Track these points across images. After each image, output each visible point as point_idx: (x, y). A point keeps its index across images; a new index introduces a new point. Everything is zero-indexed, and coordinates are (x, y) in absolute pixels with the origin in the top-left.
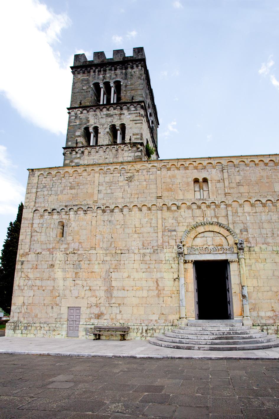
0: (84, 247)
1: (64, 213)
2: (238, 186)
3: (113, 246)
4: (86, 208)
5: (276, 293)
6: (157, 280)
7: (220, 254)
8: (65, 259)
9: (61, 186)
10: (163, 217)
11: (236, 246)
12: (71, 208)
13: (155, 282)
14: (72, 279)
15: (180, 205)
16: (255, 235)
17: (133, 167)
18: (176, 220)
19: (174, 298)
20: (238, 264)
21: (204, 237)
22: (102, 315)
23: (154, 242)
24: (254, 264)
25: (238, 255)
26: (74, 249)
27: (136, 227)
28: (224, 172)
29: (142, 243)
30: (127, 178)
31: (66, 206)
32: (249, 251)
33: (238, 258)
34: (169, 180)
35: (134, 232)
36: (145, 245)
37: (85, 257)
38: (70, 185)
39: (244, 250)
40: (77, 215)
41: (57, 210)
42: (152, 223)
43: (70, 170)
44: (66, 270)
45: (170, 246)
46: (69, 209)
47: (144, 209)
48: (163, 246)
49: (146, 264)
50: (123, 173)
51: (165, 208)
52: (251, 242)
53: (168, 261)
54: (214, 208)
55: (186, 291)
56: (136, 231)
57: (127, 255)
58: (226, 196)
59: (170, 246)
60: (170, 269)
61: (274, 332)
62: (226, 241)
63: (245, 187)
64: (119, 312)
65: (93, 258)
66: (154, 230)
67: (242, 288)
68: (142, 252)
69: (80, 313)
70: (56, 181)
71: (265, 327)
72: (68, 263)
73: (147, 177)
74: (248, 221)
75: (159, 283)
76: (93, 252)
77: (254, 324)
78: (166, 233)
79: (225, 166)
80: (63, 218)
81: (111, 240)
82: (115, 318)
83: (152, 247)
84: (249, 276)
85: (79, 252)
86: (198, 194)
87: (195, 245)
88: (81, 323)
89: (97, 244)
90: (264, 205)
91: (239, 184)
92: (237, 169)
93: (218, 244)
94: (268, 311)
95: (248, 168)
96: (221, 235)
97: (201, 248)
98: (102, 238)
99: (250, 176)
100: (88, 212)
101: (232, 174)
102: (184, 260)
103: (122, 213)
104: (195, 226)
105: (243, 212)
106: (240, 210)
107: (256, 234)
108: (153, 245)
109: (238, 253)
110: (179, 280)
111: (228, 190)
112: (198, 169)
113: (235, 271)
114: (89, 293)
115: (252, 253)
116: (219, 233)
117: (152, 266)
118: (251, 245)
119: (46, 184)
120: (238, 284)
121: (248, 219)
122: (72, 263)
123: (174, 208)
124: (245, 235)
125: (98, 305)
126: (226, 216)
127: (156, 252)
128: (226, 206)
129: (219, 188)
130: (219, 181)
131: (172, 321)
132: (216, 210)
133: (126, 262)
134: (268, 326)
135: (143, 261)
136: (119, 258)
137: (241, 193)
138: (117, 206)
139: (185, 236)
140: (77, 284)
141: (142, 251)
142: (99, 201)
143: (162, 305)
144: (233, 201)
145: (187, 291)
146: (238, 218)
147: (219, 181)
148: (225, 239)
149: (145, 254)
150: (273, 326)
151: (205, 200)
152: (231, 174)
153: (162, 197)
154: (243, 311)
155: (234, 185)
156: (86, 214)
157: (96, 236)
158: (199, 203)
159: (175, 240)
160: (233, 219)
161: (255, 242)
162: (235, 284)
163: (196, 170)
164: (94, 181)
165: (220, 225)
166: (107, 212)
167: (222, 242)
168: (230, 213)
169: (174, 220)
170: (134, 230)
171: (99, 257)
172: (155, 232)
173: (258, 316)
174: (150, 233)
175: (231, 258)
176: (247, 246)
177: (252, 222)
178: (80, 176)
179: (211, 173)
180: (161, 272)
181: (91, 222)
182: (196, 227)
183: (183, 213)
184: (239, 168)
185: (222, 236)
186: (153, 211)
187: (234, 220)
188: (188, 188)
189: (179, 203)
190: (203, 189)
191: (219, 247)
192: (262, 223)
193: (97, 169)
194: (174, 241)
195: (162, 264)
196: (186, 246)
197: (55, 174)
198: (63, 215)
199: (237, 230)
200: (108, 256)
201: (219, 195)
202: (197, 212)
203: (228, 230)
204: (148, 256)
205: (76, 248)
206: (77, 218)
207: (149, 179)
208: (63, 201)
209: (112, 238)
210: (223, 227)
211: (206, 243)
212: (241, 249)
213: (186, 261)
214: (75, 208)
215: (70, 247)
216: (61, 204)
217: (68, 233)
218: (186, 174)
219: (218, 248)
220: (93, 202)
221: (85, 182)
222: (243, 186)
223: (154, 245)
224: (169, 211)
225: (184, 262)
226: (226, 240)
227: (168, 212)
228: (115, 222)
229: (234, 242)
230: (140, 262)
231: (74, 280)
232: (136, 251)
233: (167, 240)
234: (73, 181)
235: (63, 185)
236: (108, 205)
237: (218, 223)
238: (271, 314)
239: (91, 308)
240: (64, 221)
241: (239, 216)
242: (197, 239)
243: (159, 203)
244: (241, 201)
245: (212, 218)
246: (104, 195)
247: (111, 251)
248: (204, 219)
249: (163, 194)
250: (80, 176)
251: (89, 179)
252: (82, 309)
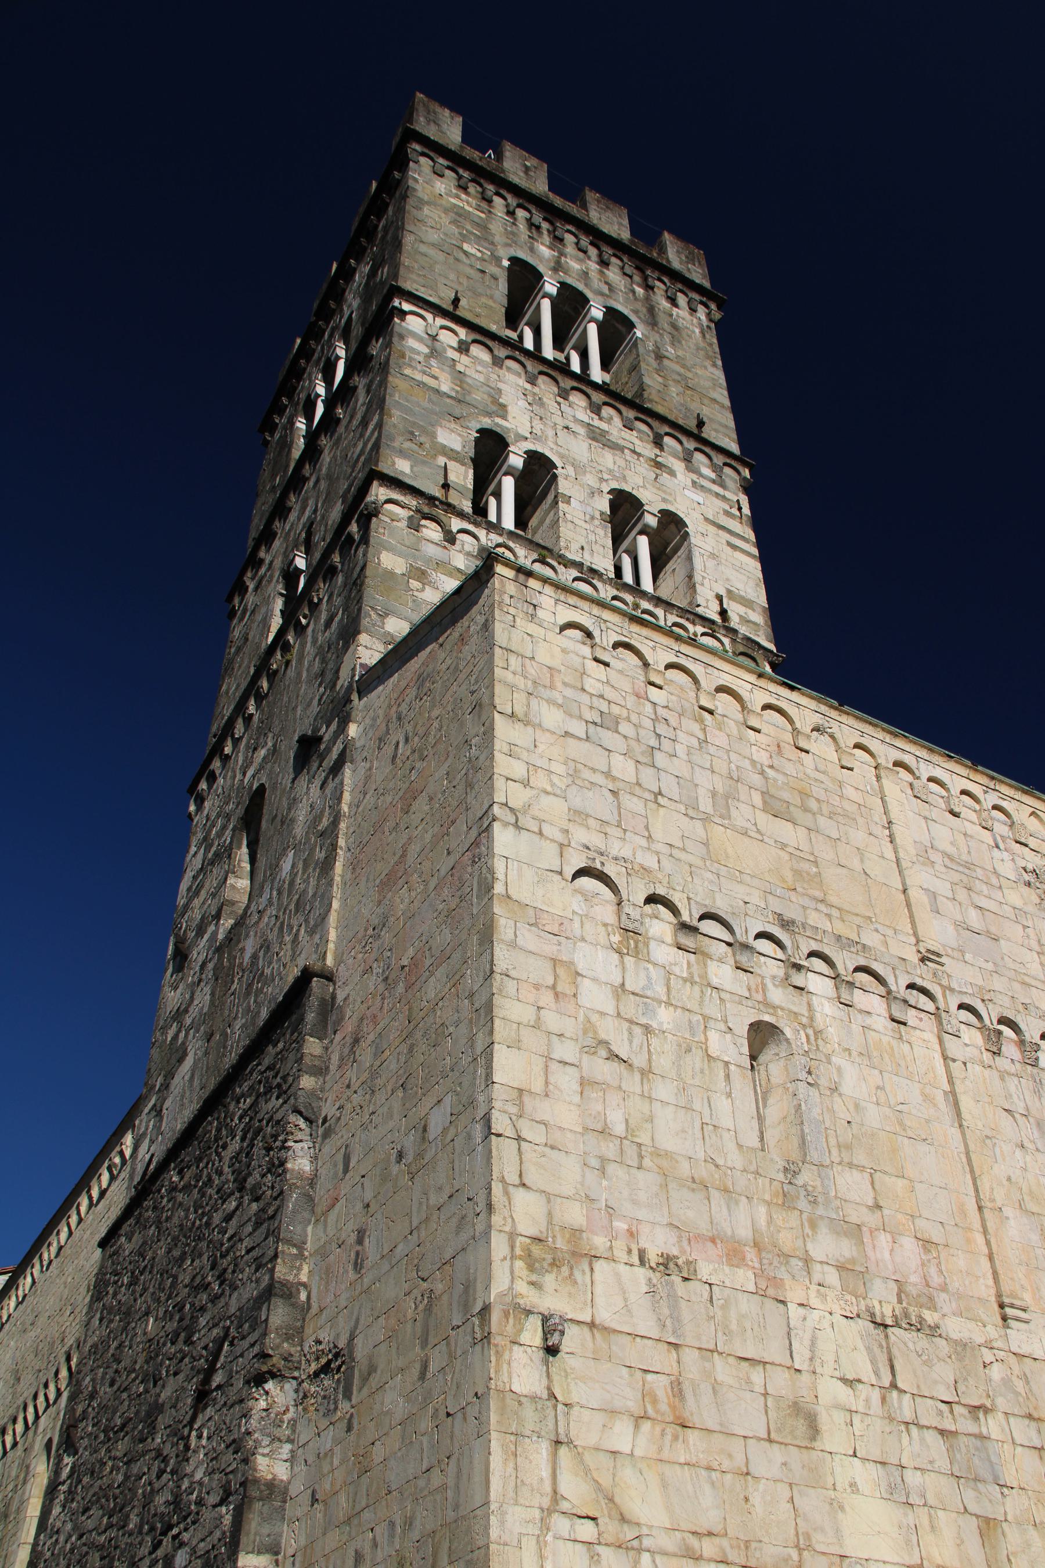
119: (616, 710)
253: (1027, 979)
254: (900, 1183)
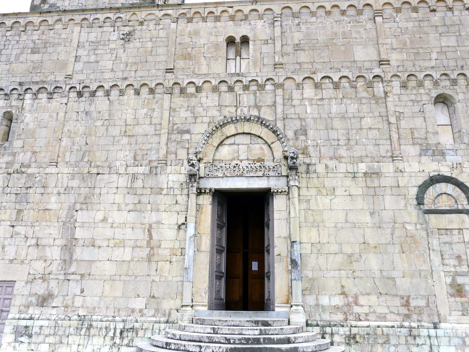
0: (39, 160)
1: (16, 96)
2: (296, 50)
3: (86, 160)
4: (53, 88)
5: (350, 256)
6: (150, 226)
7: (258, 178)
8: (3, 185)
9: (17, 47)
10: (173, 106)
11: (285, 163)
12: (27, 87)
13: (146, 230)
14: (9, 223)
15: (200, 85)
16: (319, 142)
17: (134, 16)
18: (192, 113)
19: (175, 264)
20: (288, 197)
21: (234, 144)
22: (50, 297)
23: (153, 152)
24: (313, 197)
25: (288, 179)
26: (22, 165)
27: (126, 125)
28: (275, 25)
29: (133, 155)
30: (123, 35)
31: (21, 84)
32: (308, 172)
33: (287, 186)
34: (187, 40)
35: (122, 133)
36: (138, 158)
37: (37, 179)
38: (32, 45)
39: (299, 171)
40: (37, 101)
41: (5, 91)
42: (154, 116)
43: (36, 19)
44: (4, 204)
45: (177, 162)
46: (24, 89)
47: (145, 91)
48: (166, 161)
49: (136, 194)
50: (118, 27)
51: (177, 90)
52: (311, 155)
53: (172, 190)
54: (255, 91)
55: (196, 250)
56: (126, 132)
57: (106, 177)
58: (275, 68)
59: (177, 162)
60: (173, 206)
61: (343, 340)
62: (270, 152)
63: (307, 52)
64: (80, 292)
65: (52, 182)
66: (155, 130)
67: (292, 246)
68: (131, 172)
69: (11, 294)
70: (10, 38)
71: (328, 330)
72: (8, 191)
73: (154, 33)
74: (308, 115)
75: (152, 233)
76: (53, 170)
77: (309, 322)
78: (175, 135)
79: (277, 14)
80: (12, 106)
81: (84, 148)
82: (71, 304)
83: (150, 161)
84: (305, 222)
85: (30, 171)
86: (232, 64)
87: (218, 160)
88: (10, 316)
89: (61, 155)
90: (336, 86)
91: (298, 48)
92: (297, 21)
93: (256, 158)
94: (335, 294)
95: (314, 19)
96: (262, 140)
97: (228, 166)
98: (70, 144)
99: (316, 32)
100: (55, 96)
101: (288, 30)
102: (198, 188)
103: (109, 99)
104: (221, 124)
105: (301, 98)
106: (296, 94)
107: (320, 140)
108: (150, 159)
109: (287, 176)
110: (186, 227)
111: (279, 58)
112: (236, 20)
113: (281, 212)
114: (34, 253)
115: (312, 176)
116: (259, 137)
117: (144, 199)
118: (311, 160)
120: (285, 238)
121: (309, 111)
122: (14, 191)
123: (191, 90)
124: (302, 141)
125: (47, 276)
126: (273, 105)
127: (154, 173)
128: (275, 87)
129: (266, 55)
130: (266, 42)
131: (167, 313)
132: (258, 94)
133: (104, 191)
134: (333, 328)
135: (131, 190)
136: (93, 183)
137: (300, 63)
138: (101, 85)
139: (204, 142)
140: (18, 234)
141: (131, 170)
142: (74, 76)
143: (154, 278)
144: (285, 77)
145: (198, 250)
146: (293, 110)
147: (266, 42)
148: (268, 148)
149: (136, 175)
150: (343, 326)
151: (242, 76)
152: (287, 28)
153: (175, 71)
154: (292, 293)
155: (289, 49)
156: (51, 100)
157: (62, 139)
158: (231, 81)
159: (186, 150)
160: (283, 111)
161: (318, 156)
162: (280, 237)
163: (231, 23)
164: (71, 40)
165: (262, 123)
166: (85, 96)
167: (264, 155)
168: (279, 100)
169: (189, 112)
170: (123, 129)
171: (60, 180)
172: (156, 135)
173: (317, 305)
174: (149, 137)
175: (276, 186)
176: (304, 162)
177: (316, 116)
178: (50, 30)
179: (255, 28)
180: (158, 210)
181: (58, 113)
182: (223, 126)
183: (204, 100)
184: (300, 18)
185: (264, 142)
186: (157, 95)
187: (285, 113)
188: (216, 53)
189: (198, 82)
190: (240, 57)
191: (257, 163)
192: (331, 118)
193: (78, 18)
194: (185, 152)
195: (162, 196)
196: (204, 161)
197: (10, 25)
198: (13, 101)
199: (290, 131)
200: (76, 178)
201: (265, 66)
202: (228, 98)
203: (274, 132)
204: (141, 180)
205: (27, 162)
206: (35, 105)
207: (156, 38)
208: (17, 75)
209: (87, 144)
210: (267, 127)
211: (236, 155)
212: (294, 169)
213: (201, 189)
214: (35, 88)
215: (16, 161)
216: (14, 79)
217: (16, 135)
218: (215, 29)
219: (255, 165)
220: (66, 78)
221: (56, 41)
222: (303, 50)
223: (153, 159)
224: (182, 95)
225: (198, 192)
226: (270, 149)
227: (180, 96)
228: (95, 115)
229: (283, 154)
230: (126, 191)
231: (13, 226)
232: (122, 171)
233: (173, 149)
234: (38, 39)
235: (21, 46)
236: (87, 83)
237: (259, 118)
238: (338, 301)
239: (33, 284)
240: (14, 112)
241: (295, 106)
242: (222, 147)
243: (169, 80)
244: (299, 79)
245: (251, 109)
246: (84, 65)
247: (82, 169)
248: (236, 111)
249: (175, 65)
250: (50, 30)
251: (64, 36)
252: (17, 285)
253: (104, 71)
254: (32, 139)
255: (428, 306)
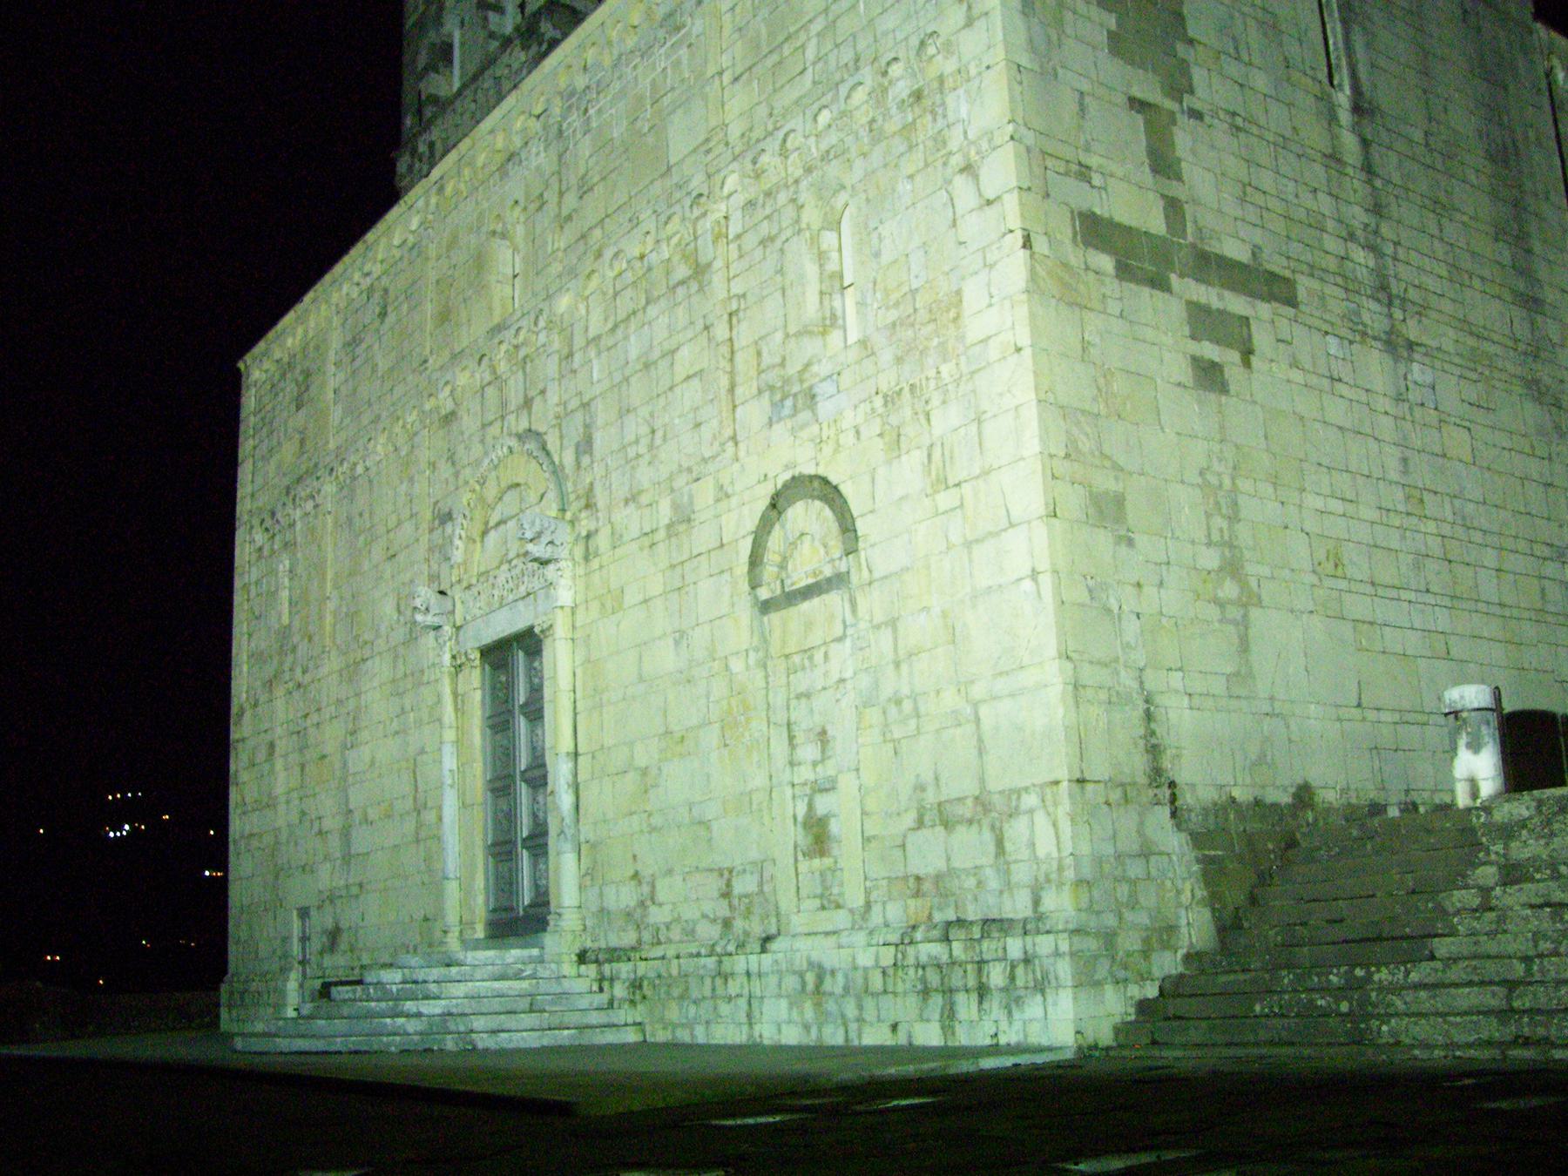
255: (762, 892)
